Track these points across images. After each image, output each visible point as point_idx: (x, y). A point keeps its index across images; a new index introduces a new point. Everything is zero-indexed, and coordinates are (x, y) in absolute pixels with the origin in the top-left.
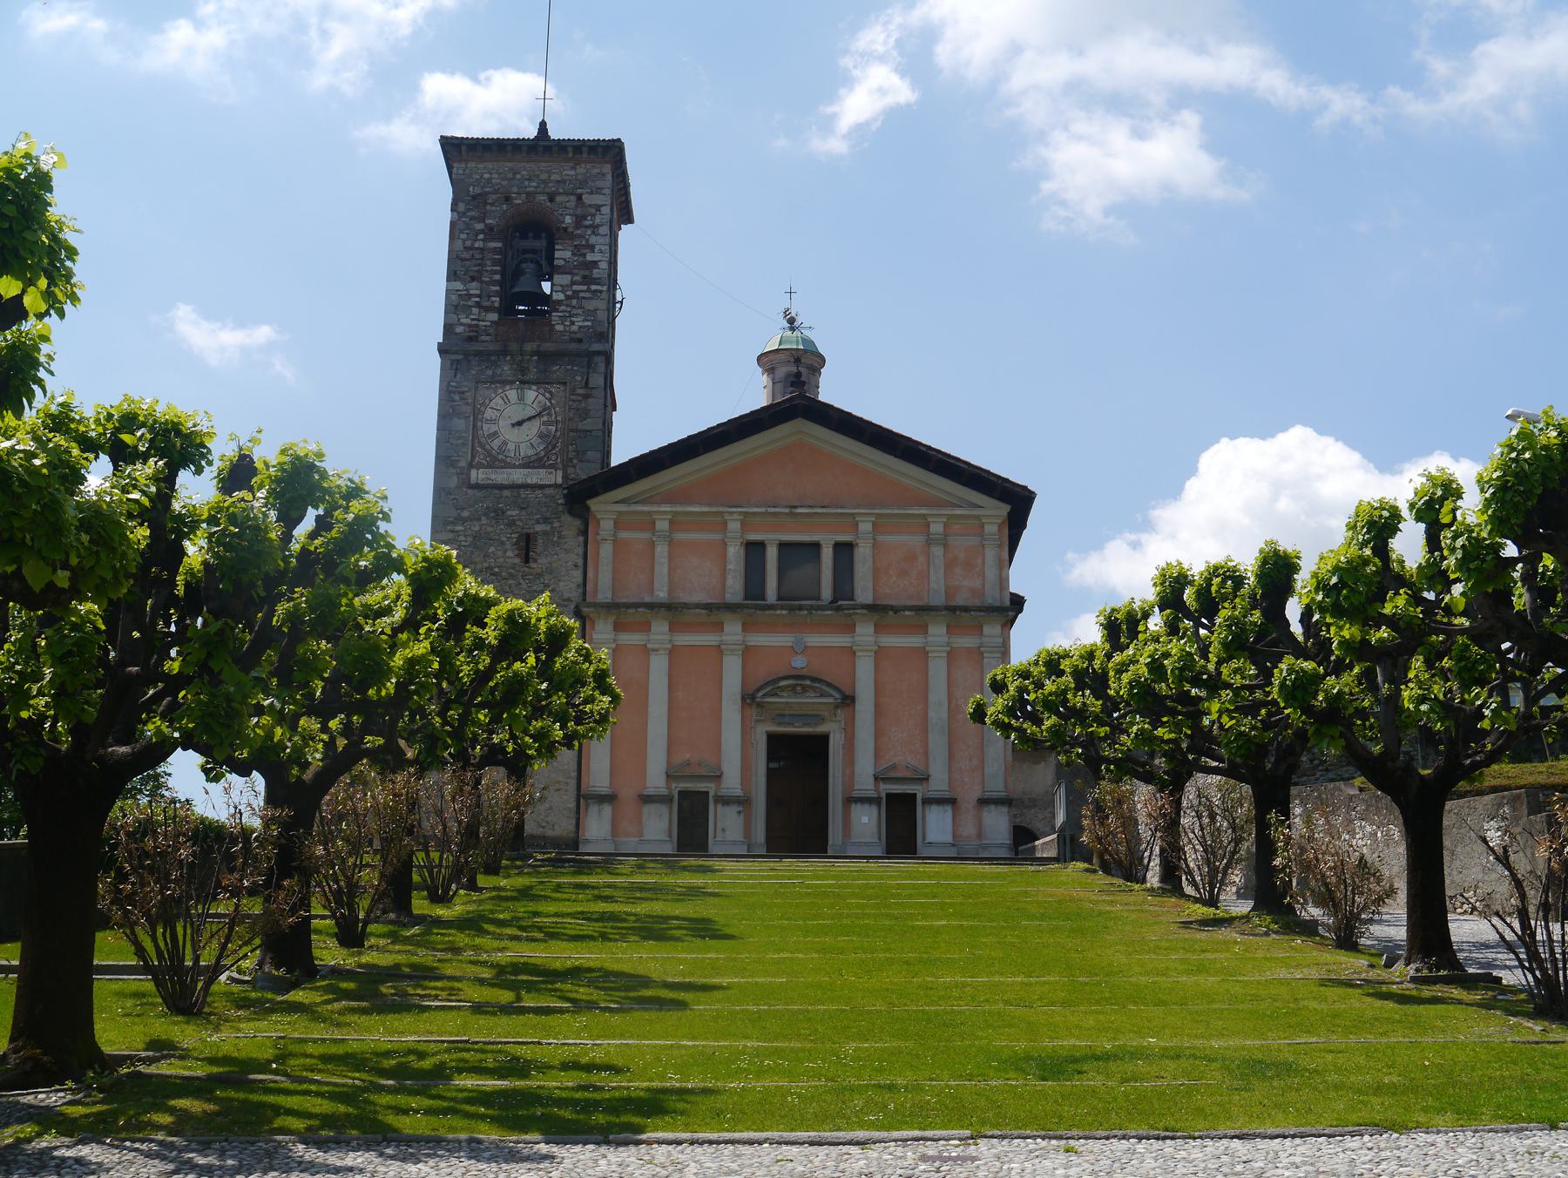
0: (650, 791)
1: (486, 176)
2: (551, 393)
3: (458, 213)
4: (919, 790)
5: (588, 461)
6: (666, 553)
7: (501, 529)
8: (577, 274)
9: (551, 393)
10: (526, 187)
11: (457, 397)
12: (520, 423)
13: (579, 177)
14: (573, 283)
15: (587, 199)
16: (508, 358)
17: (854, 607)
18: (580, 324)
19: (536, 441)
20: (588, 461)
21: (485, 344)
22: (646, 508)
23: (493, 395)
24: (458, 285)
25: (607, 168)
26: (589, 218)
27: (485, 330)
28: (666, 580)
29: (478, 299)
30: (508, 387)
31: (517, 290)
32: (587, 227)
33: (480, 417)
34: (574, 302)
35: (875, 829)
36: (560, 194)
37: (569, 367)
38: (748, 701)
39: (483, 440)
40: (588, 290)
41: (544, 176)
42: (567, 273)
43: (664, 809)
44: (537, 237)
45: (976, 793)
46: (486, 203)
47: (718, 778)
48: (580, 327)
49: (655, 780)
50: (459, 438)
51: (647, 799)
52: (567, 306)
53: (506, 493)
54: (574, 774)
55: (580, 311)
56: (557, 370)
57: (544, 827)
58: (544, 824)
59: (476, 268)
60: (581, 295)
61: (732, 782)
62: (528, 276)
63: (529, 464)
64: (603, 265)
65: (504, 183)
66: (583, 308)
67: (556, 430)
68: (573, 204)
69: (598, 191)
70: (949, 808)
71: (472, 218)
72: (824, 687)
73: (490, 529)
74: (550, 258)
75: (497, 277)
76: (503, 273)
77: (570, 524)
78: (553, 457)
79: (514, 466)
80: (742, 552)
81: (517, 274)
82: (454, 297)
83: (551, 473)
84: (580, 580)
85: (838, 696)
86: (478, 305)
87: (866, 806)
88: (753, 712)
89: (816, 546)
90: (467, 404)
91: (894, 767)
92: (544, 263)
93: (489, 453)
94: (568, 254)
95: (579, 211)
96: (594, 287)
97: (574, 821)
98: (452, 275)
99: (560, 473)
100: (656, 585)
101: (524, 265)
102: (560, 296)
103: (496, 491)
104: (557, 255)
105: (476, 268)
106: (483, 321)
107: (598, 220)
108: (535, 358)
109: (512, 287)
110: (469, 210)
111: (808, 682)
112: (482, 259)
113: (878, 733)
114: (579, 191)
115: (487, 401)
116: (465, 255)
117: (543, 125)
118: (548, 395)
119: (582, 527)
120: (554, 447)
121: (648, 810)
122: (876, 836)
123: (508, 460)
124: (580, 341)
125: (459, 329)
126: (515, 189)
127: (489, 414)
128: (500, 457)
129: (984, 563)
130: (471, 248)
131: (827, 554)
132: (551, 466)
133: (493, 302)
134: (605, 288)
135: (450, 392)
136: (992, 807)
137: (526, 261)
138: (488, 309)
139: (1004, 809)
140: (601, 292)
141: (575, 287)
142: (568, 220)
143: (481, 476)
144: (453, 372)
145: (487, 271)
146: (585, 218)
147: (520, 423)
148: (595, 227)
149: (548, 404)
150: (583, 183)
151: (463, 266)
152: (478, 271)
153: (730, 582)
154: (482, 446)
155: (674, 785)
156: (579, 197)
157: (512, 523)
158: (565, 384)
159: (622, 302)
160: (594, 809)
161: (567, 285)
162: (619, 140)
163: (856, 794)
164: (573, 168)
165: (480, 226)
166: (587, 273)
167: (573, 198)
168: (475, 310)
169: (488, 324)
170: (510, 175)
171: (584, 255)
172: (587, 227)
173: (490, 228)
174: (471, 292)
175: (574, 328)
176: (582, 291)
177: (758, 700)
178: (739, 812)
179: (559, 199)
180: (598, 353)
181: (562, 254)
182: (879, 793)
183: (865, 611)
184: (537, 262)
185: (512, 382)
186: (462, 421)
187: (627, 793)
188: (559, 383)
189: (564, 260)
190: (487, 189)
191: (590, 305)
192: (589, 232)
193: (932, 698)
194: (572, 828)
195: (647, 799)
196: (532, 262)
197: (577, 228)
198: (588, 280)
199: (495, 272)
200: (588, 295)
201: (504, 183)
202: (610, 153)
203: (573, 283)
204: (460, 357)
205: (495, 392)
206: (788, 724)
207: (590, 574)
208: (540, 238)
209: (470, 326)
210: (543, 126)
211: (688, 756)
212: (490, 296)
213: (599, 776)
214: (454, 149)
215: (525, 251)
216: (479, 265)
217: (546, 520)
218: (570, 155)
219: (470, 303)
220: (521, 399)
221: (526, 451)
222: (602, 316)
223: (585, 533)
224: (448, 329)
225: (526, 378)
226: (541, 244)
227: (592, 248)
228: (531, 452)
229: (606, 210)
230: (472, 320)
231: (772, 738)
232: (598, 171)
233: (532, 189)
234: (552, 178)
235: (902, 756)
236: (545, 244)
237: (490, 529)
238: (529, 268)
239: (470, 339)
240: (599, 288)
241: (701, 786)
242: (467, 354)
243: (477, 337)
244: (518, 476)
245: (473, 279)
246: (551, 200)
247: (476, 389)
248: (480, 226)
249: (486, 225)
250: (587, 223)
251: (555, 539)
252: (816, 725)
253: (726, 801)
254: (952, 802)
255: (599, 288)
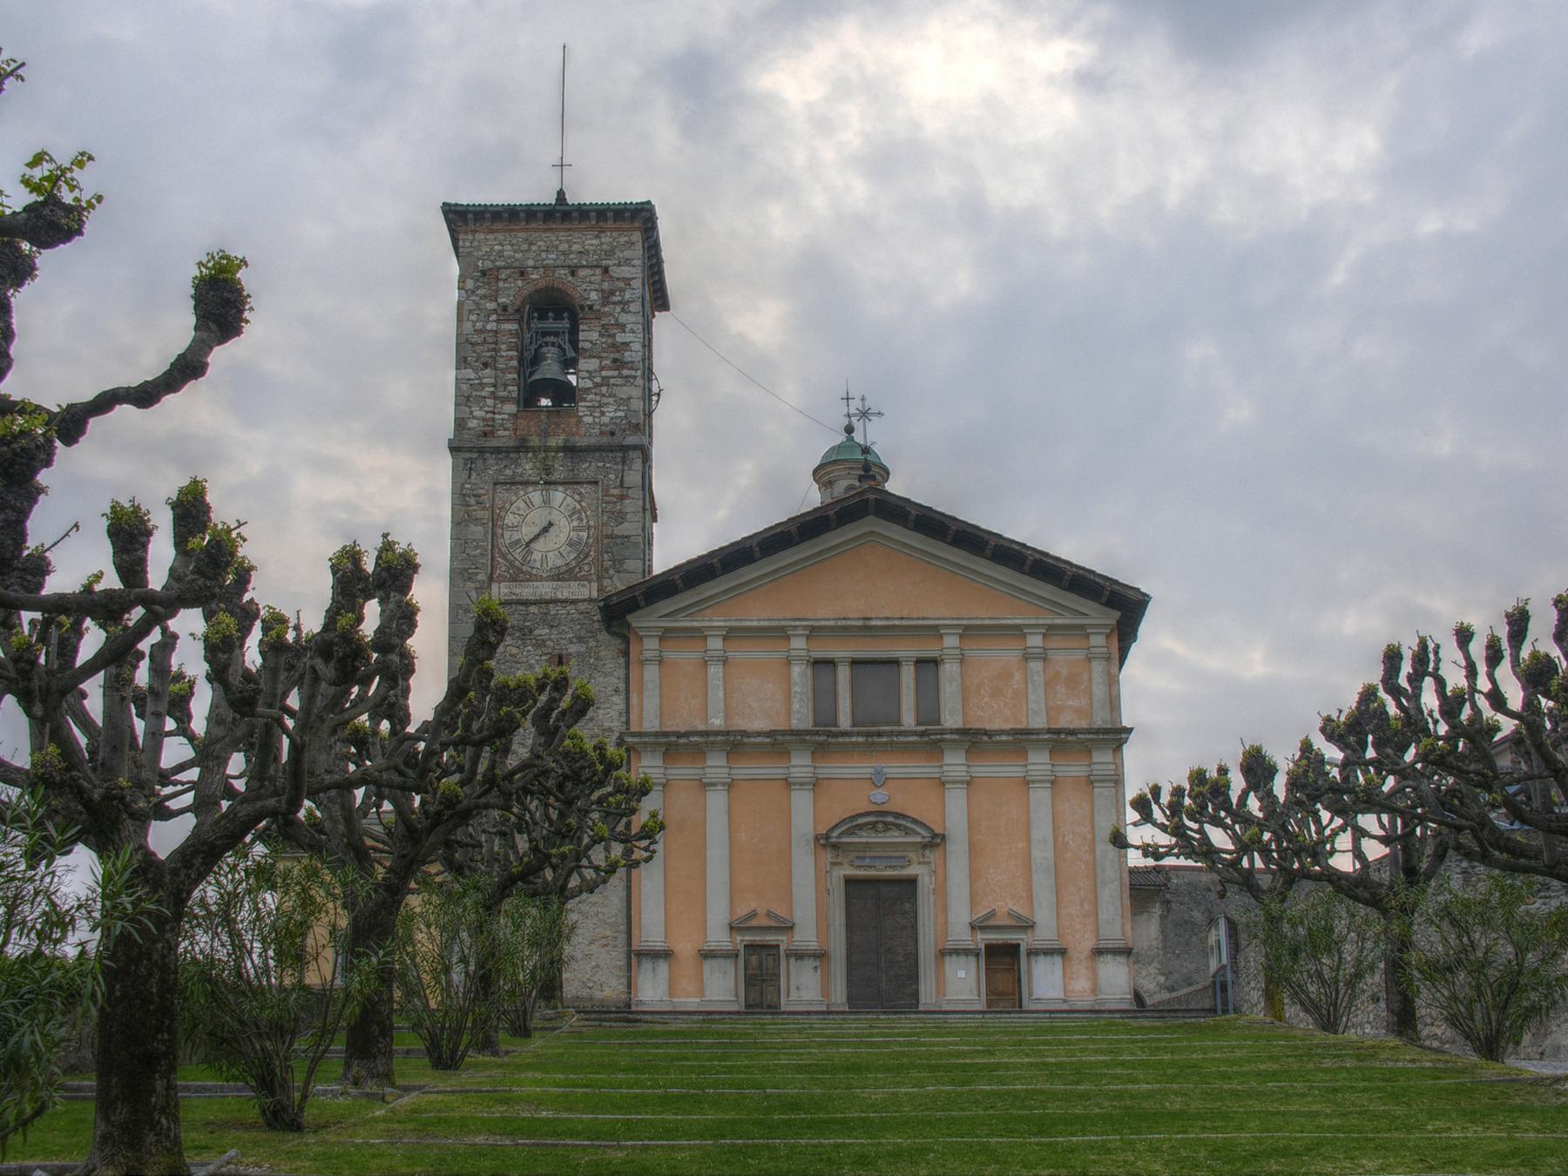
0: (713, 946)
1: (497, 248)
2: (580, 494)
3: (467, 291)
4: (1024, 940)
5: (627, 571)
6: (721, 674)
7: (528, 651)
8: (606, 358)
9: (580, 494)
10: (543, 260)
11: (472, 501)
12: (545, 530)
13: (604, 247)
14: (602, 368)
15: (616, 272)
16: (530, 455)
17: (943, 732)
18: (612, 414)
19: (565, 549)
20: (627, 571)
21: (504, 440)
22: (695, 624)
23: (514, 498)
24: (469, 373)
25: (637, 236)
26: (618, 293)
27: (502, 425)
28: (722, 704)
29: (492, 389)
30: (531, 489)
31: (536, 377)
32: (615, 303)
33: (500, 523)
34: (604, 389)
35: (974, 985)
36: (583, 266)
37: (599, 464)
38: (822, 842)
39: (503, 549)
40: (620, 376)
41: (564, 247)
42: (594, 357)
43: (729, 965)
44: (558, 317)
45: (1088, 944)
46: (498, 279)
47: (789, 928)
48: (612, 418)
49: (718, 937)
50: (476, 548)
51: (707, 955)
52: (596, 394)
53: (533, 609)
54: (623, 928)
55: (611, 400)
56: (587, 469)
57: (590, 988)
58: (590, 985)
59: (489, 354)
60: (612, 381)
61: (806, 936)
62: (549, 361)
63: (559, 576)
64: (637, 347)
65: (519, 256)
66: (615, 396)
67: (588, 538)
68: (598, 278)
69: (627, 262)
70: (1058, 959)
71: (484, 297)
72: (909, 825)
73: (515, 651)
74: (574, 343)
75: (515, 363)
76: (521, 360)
77: (608, 647)
78: (586, 568)
79: (541, 579)
80: (809, 672)
81: (536, 360)
82: (464, 387)
83: (584, 586)
84: (623, 706)
85: (924, 833)
86: (494, 396)
87: (963, 958)
88: (828, 856)
89: (895, 663)
90: (484, 509)
91: (992, 914)
92: (567, 346)
93: (512, 565)
94: (595, 336)
95: (606, 286)
96: (625, 372)
97: (624, 981)
98: (462, 362)
99: (595, 585)
100: (711, 711)
101: (545, 350)
102: (589, 384)
103: (521, 608)
104: (581, 336)
105: (489, 354)
106: (499, 413)
107: (627, 296)
108: (561, 454)
109: (531, 374)
110: (478, 288)
111: (890, 819)
112: (496, 343)
113: (974, 875)
114: (604, 263)
115: (507, 505)
116: (476, 339)
117: (561, 194)
118: (577, 497)
119: (622, 646)
120: (587, 556)
121: (708, 965)
122: (975, 992)
123: (534, 572)
124: (612, 434)
125: (473, 424)
126: (531, 263)
127: (510, 519)
128: (524, 568)
129: (1090, 680)
130: (482, 331)
131: (908, 674)
132: (584, 578)
133: (509, 392)
134: (639, 373)
135: (465, 495)
136: (1110, 957)
137: (546, 344)
138: (504, 400)
139: (1122, 959)
140: (635, 377)
141: (604, 373)
142: (594, 296)
143: (504, 590)
144: (467, 472)
145: (502, 357)
146: (612, 293)
147: (545, 530)
148: (624, 304)
149: (578, 507)
150: (610, 253)
151: (474, 352)
152: (491, 357)
153: (796, 706)
154: (504, 557)
155: (739, 938)
156: (606, 270)
157: (540, 644)
158: (596, 483)
159: (659, 395)
160: (647, 965)
161: (595, 371)
162: (649, 202)
163: (949, 945)
164: (597, 237)
165: (491, 306)
166: (617, 356)
167: (598, 271)
168: (490, 402)
169: (506, 417)
170: (525, 247)
171: (613, 336)
172: (615, 303)
173: (505, 308)
174: (484, 381)
175: (605, 420)
176: (613, 377)
177: (834, 840)
178: (816, 967)
179: (582, 273)
180: (635, 448)
181: (589, 335)
182: (977, 944)
183: (955, 737)
184: (560, 346)
185: (535, 483)
186: (480, 528)
187: (686, 948)
188: (589, 483)
189: (591, 342)
190: (497, 264)
191: (623, 392)
192: (618, 309)
193: (1036, 835)
194: (623, 988)
195: (707, 955)
196: (553, 346)
197: (604, 305)
198: (618, 364)
199: (511, 358)
200: (619, 381)
201: (519, 256)
202: (640, 218)
203: (602, 368)
204: (475, 455)
205: (516, 494)
206: (870, 867)
207: (634, 700)
208: (563, 319)
209: (484, 419)
210: (561, 194)
211: (754, 905)
212: (506, 386)
213: (651, 930)
214: (459, 218)
215: (544, 334)
216: (494, 350)
217: (580, 639)
218: (593, 222)
219: (483, 394)
220: (547, 502)
221: (554, 561)
222: (637, 405)
223: (626, 653)
224: (460, 424)
225: (552, 478)
226: (565, 324)
227: (622, 327)
228: (559, 562)
229: (637, 284)
230: (487, 412)
231: (849, 882)
232: (626, 239)
233: (552, 262)
234: (573, 249)
235: (1004, 904)
236: (568, 325)
237: (515, 651)
238: (551, 353)
239: (485, 434)
240: (633, 373)
241: (770, 938)
242: (481, 451)
243: (493, 432)
244: (545, 589)
245: (486, 365)
246: (573, 274)
247: (494, 490)
248: (491, 306)
249: (498, 305)
250: (616, 299)
251: (592, 661)
252: (902, 867)
253: (799, 956)
254: (1062, 952)
255: (633, 373)
